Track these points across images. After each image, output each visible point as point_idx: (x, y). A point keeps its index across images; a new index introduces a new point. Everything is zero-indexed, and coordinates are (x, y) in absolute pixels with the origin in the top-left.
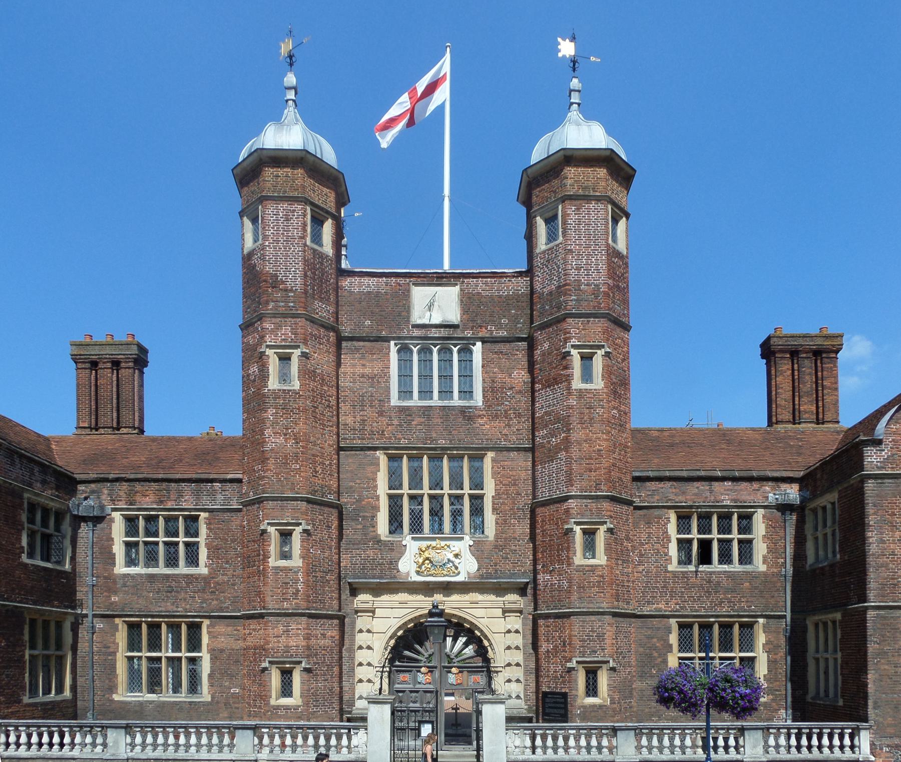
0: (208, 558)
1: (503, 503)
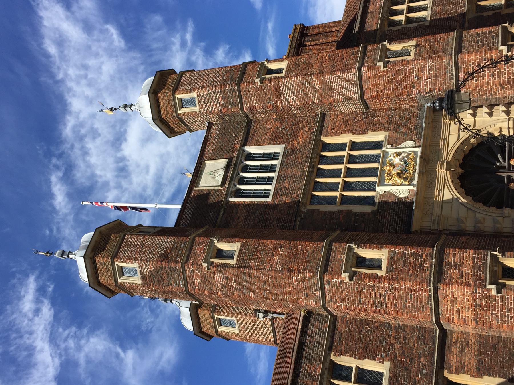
0: (373, 358)
1: (360, 128)
